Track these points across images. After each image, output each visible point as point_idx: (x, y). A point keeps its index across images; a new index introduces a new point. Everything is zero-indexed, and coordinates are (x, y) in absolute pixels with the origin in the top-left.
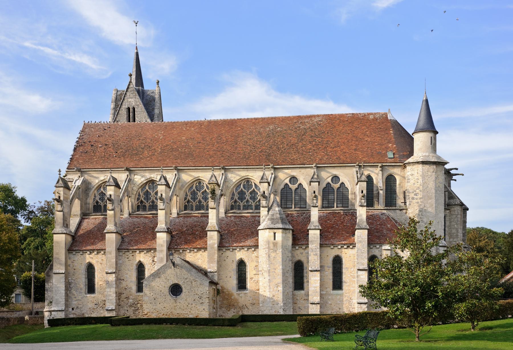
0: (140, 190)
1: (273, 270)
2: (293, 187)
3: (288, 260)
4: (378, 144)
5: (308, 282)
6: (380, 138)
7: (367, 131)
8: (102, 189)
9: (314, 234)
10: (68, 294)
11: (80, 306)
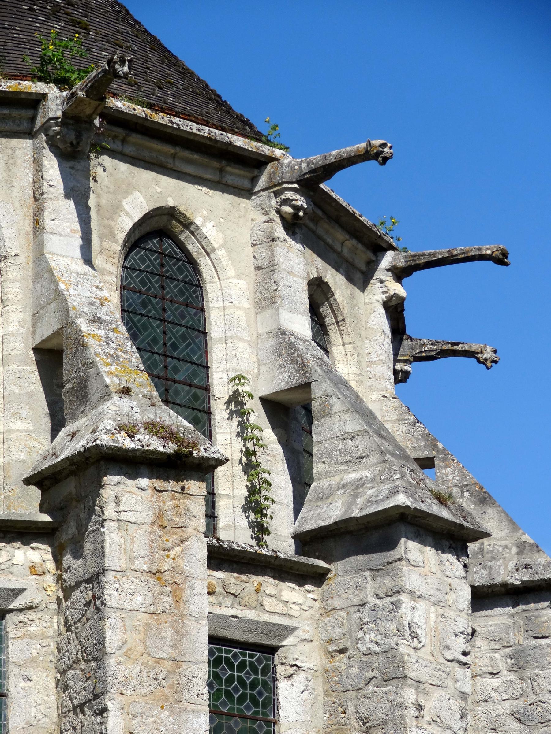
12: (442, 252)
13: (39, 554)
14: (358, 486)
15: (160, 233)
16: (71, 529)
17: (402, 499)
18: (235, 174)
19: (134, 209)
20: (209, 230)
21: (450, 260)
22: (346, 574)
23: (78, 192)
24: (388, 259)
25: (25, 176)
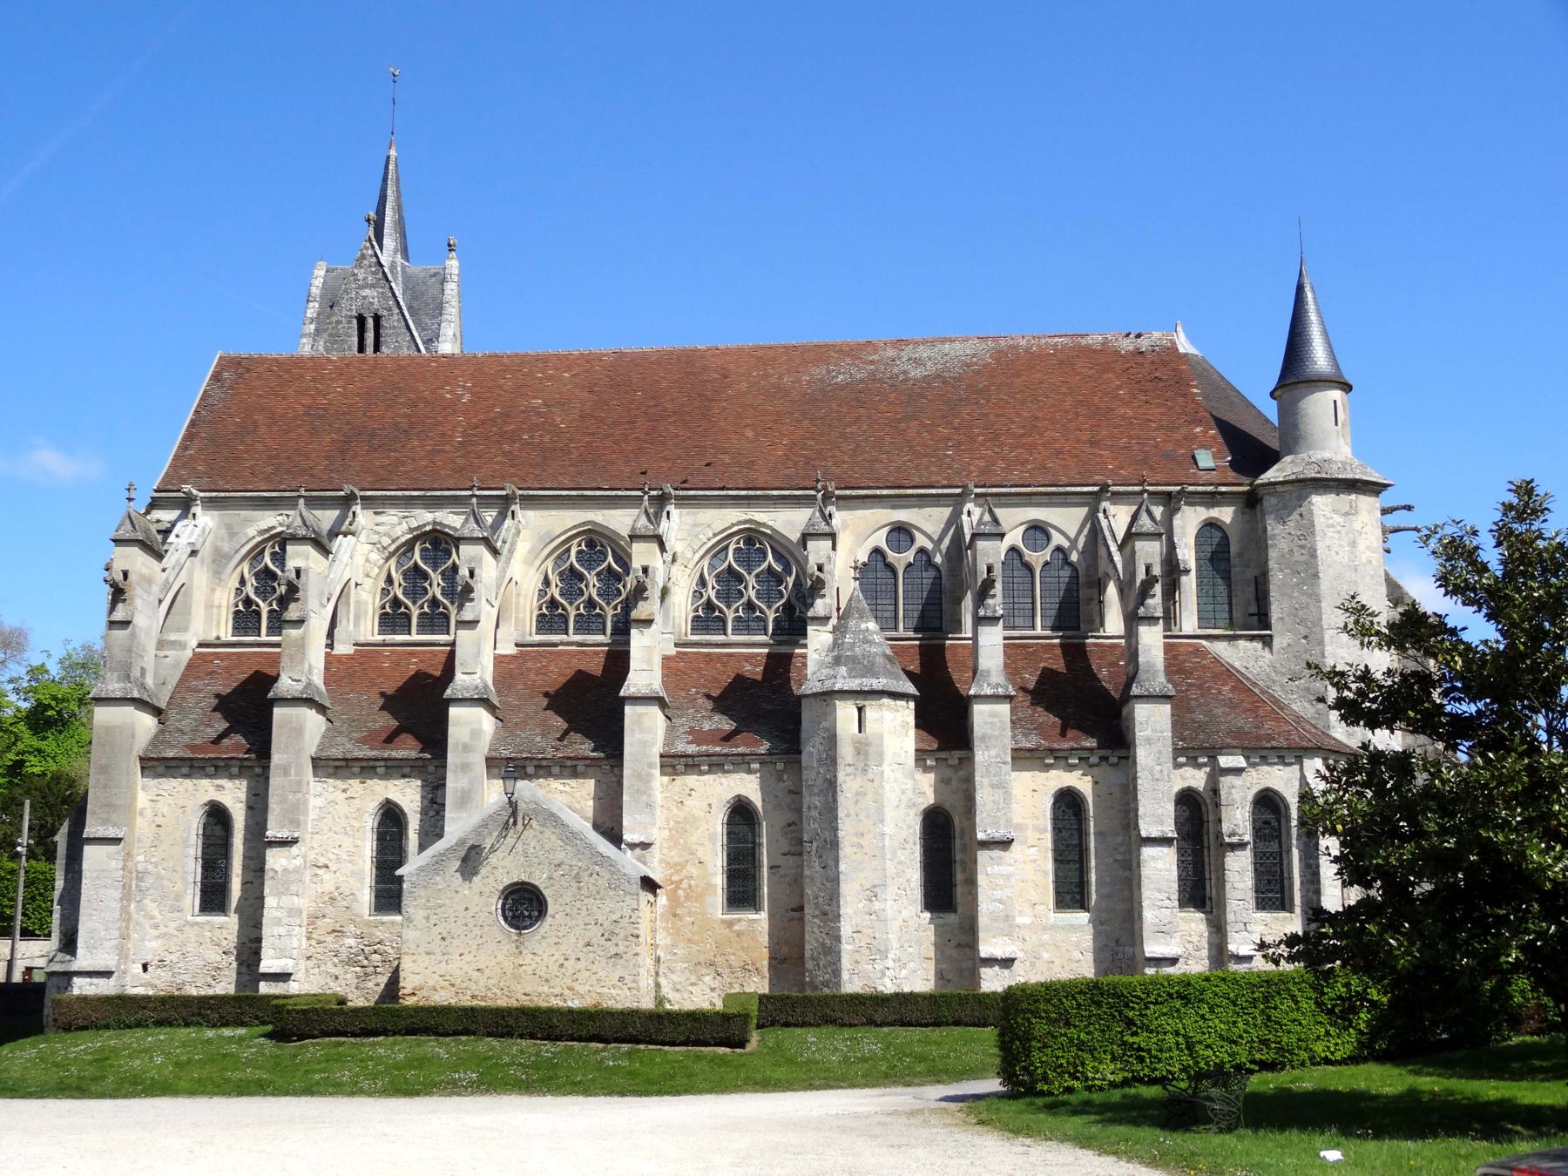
0: (393, 563)
1: (855, 840)
2: (901, 559)
3: (903, 805)
4: (1161, 427)
5: (972, 882)
6: (1163, 410)
7: (1119, 388)
8: (267, 559)
9: (992, 715)
10: (128, 913)
11: (168, 958)
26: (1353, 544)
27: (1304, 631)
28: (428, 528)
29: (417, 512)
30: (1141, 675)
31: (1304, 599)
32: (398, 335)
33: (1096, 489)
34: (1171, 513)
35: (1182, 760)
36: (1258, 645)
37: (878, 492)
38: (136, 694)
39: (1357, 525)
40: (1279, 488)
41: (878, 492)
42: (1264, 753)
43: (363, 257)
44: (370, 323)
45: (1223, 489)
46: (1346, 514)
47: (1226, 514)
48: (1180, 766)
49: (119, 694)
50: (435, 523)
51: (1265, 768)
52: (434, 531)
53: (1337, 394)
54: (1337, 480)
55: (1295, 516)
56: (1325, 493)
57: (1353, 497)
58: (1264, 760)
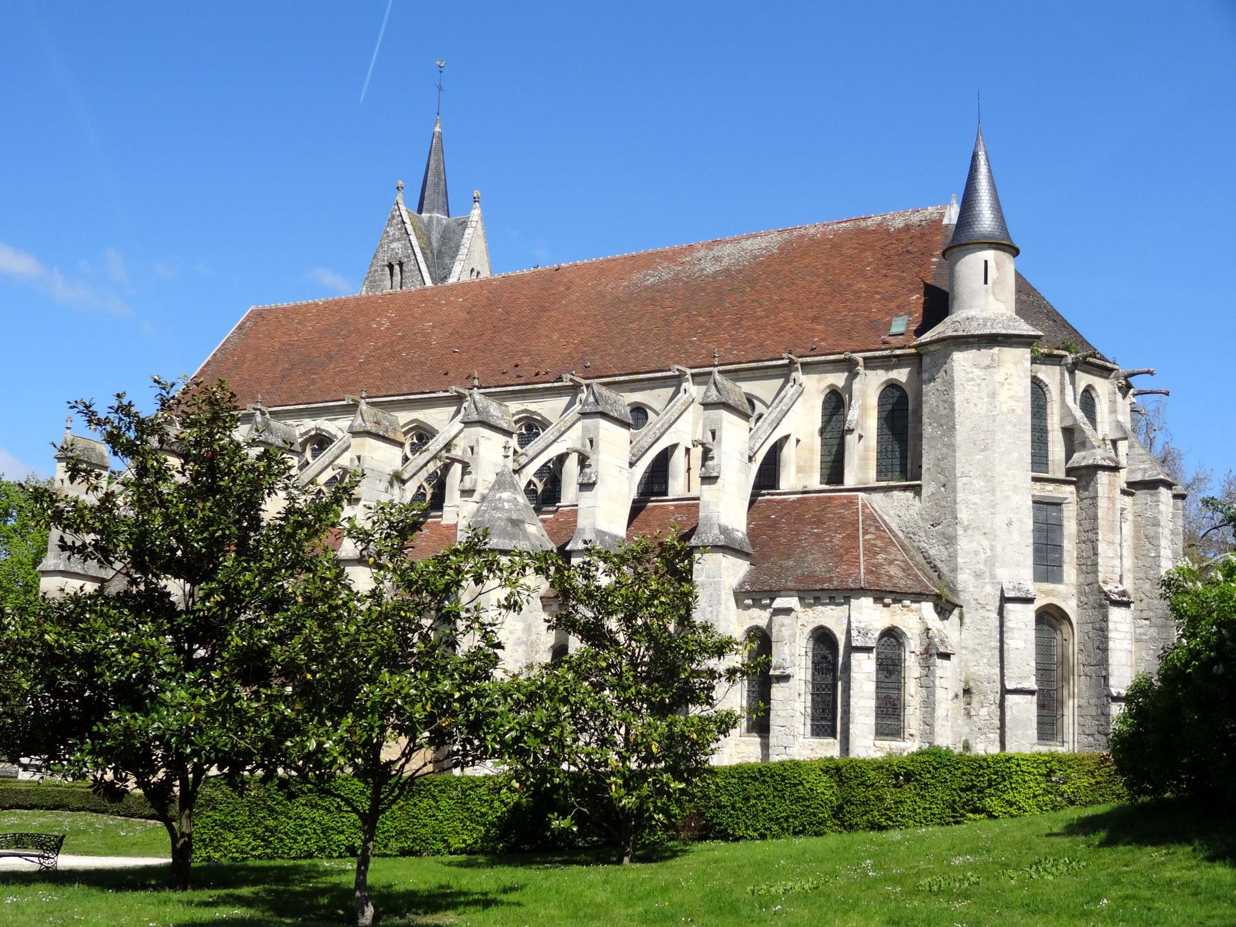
12: (1148, 389)
13: (1072, 488)
14: (1145, 470)
15: (1088, 390)
16: (1084, 483)
17: (1162, 477)
18: (1105, 374)
19: (1081, 387)
20: (1099, 390)
21: (1151, 393)
22: (1142, 495)
23: (1073, 383)
24: (1132, 391)
25: (1058, 377)
26: (993, 395)
27: (942, 479)
28: (313, 433)
29: (306, 421)
30: (701, 528)
31: (945, 450)
32: (413, 276)
33: (786, 361)
34: (853, 375)
35: (749, 602)
36: (910, 495)
37: (617, 379)
38: (62, 568)
39: (999, 375)
40: (931, 348)
41: (617, 379)
42: (818, 594)
43: (393, 217)
44: (397, 268)
45: (898, 352)
46: (989, 367)
47: (901, 375)
48: (748, 607)
49: (52, 568)
50: (317, 429)
51: (820, 608)
52: (316, 435)
53: (990, 255)
54: (973, 336)
55: (942, 373)
56: (967, 349)
57: (996, 350)
58: (817, 601)
